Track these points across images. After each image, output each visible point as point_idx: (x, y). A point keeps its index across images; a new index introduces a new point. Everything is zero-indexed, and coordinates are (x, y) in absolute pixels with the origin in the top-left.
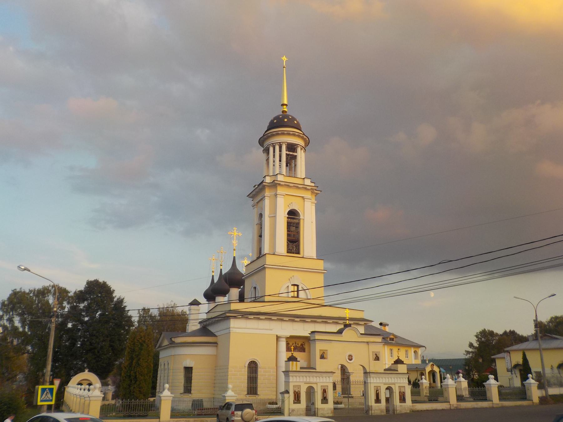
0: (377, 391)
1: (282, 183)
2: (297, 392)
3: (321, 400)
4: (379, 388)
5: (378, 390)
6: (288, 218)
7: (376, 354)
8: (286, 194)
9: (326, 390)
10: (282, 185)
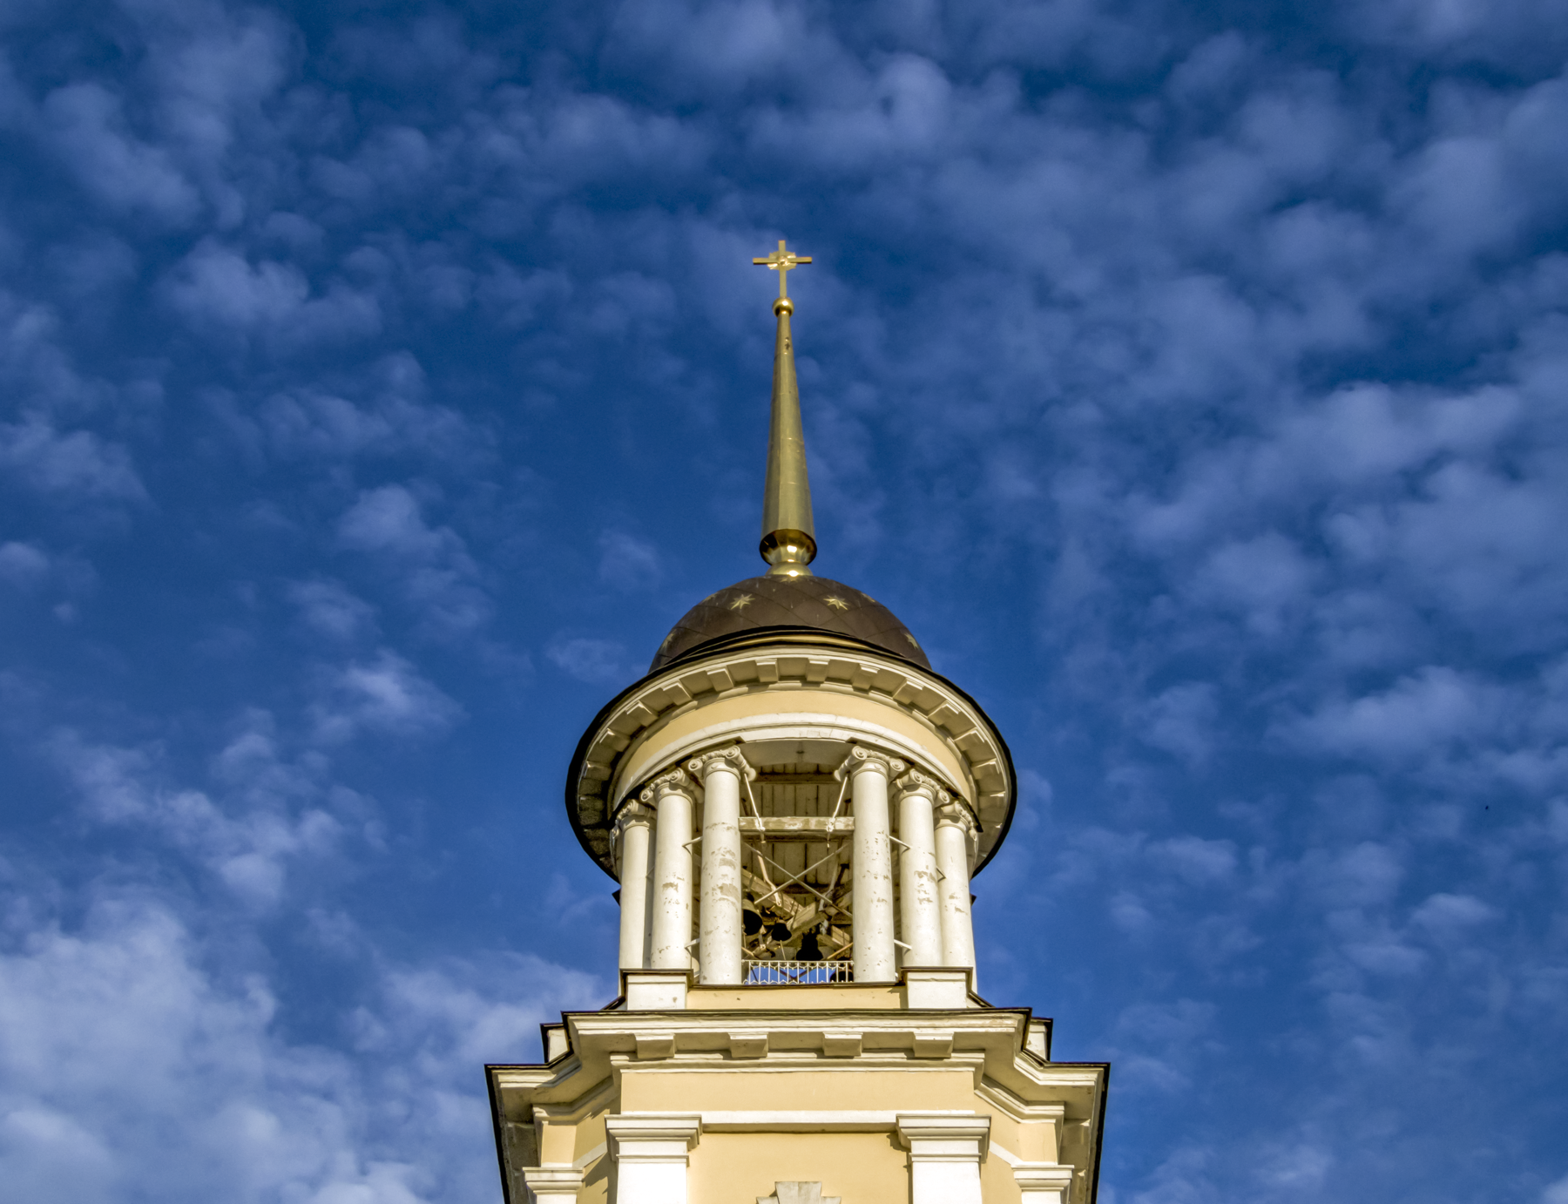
1: (647, 1032)
8: (704, 1121)
10: (659, 1053)
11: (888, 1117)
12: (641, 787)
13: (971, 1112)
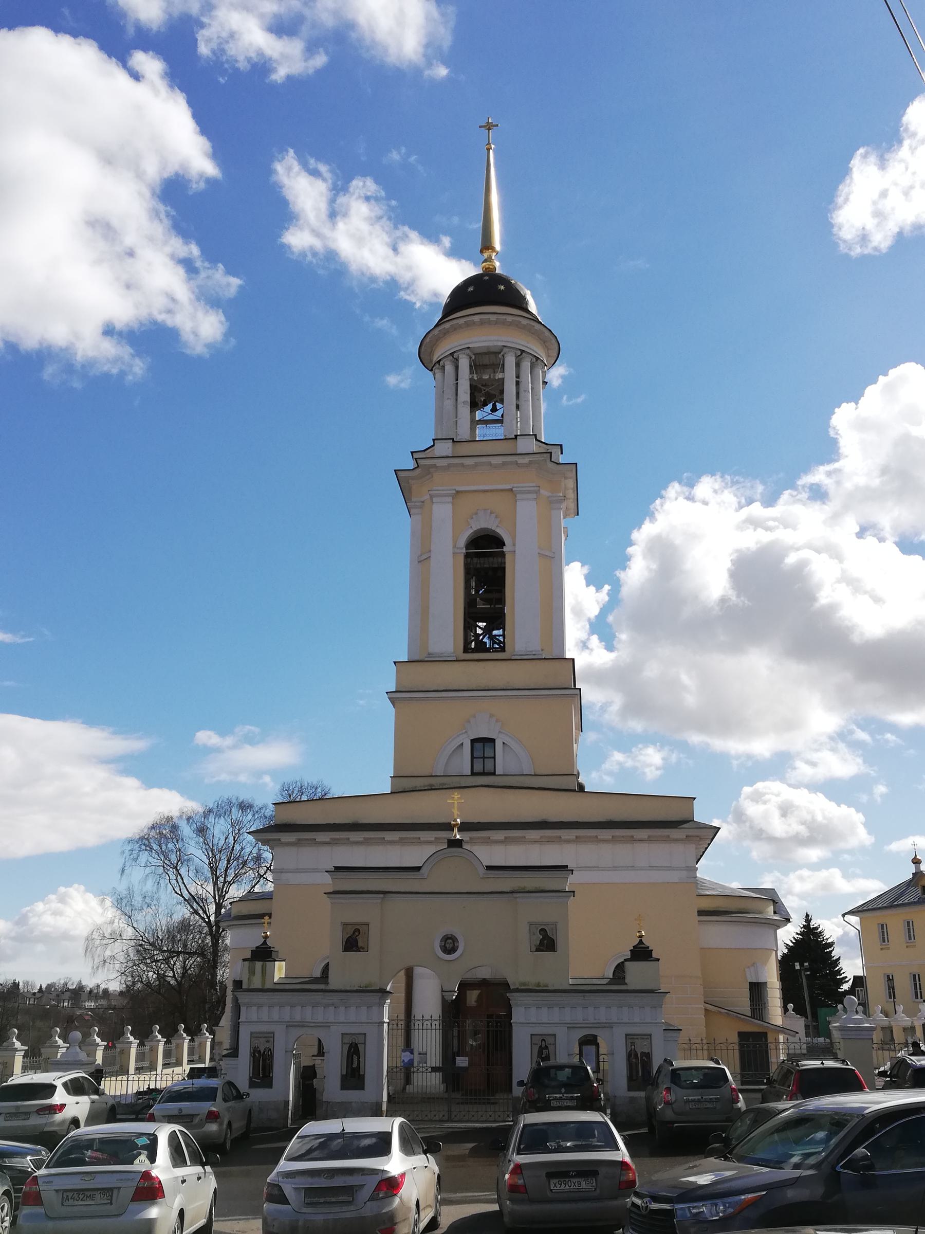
0: (541, 1050)
2: (262, 1052)
3: (343, 1076)
4: (550, 1040)
5: (546, 1047)
6: (467, 556)
7: (543, 931)
9: (361, 1047)
11: (508, 487)
12: (440, 360)
13: (534, 485)
